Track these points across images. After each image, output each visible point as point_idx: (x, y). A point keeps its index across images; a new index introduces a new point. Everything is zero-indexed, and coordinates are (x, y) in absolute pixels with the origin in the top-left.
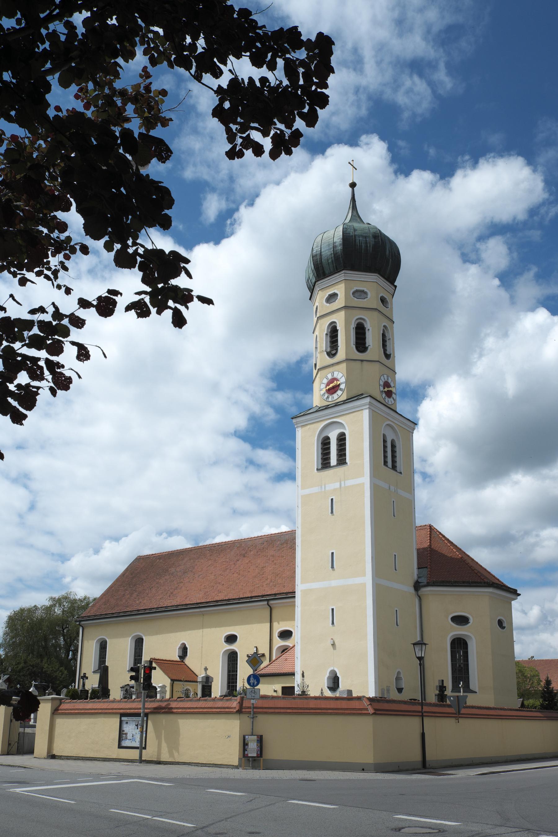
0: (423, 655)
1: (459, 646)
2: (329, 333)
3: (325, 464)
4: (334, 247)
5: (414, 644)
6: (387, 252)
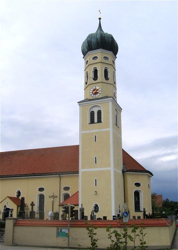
1: (137, 194)
3: (92, 122)
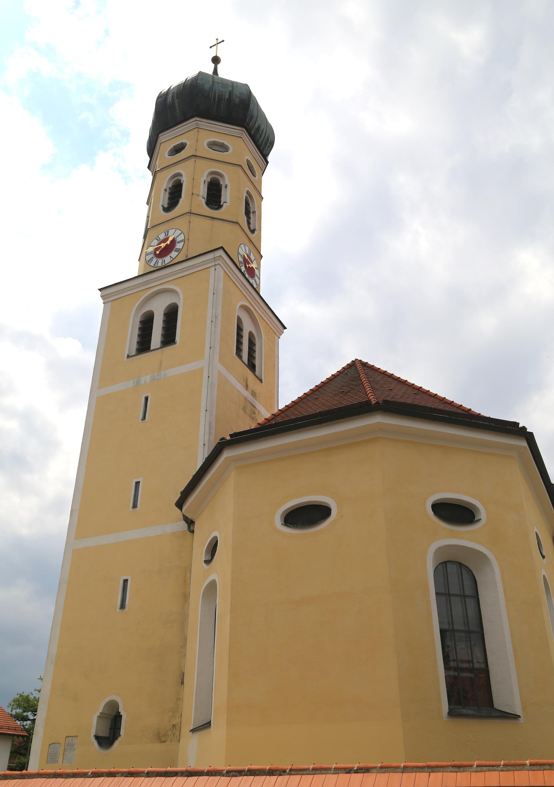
2: (168, 191)
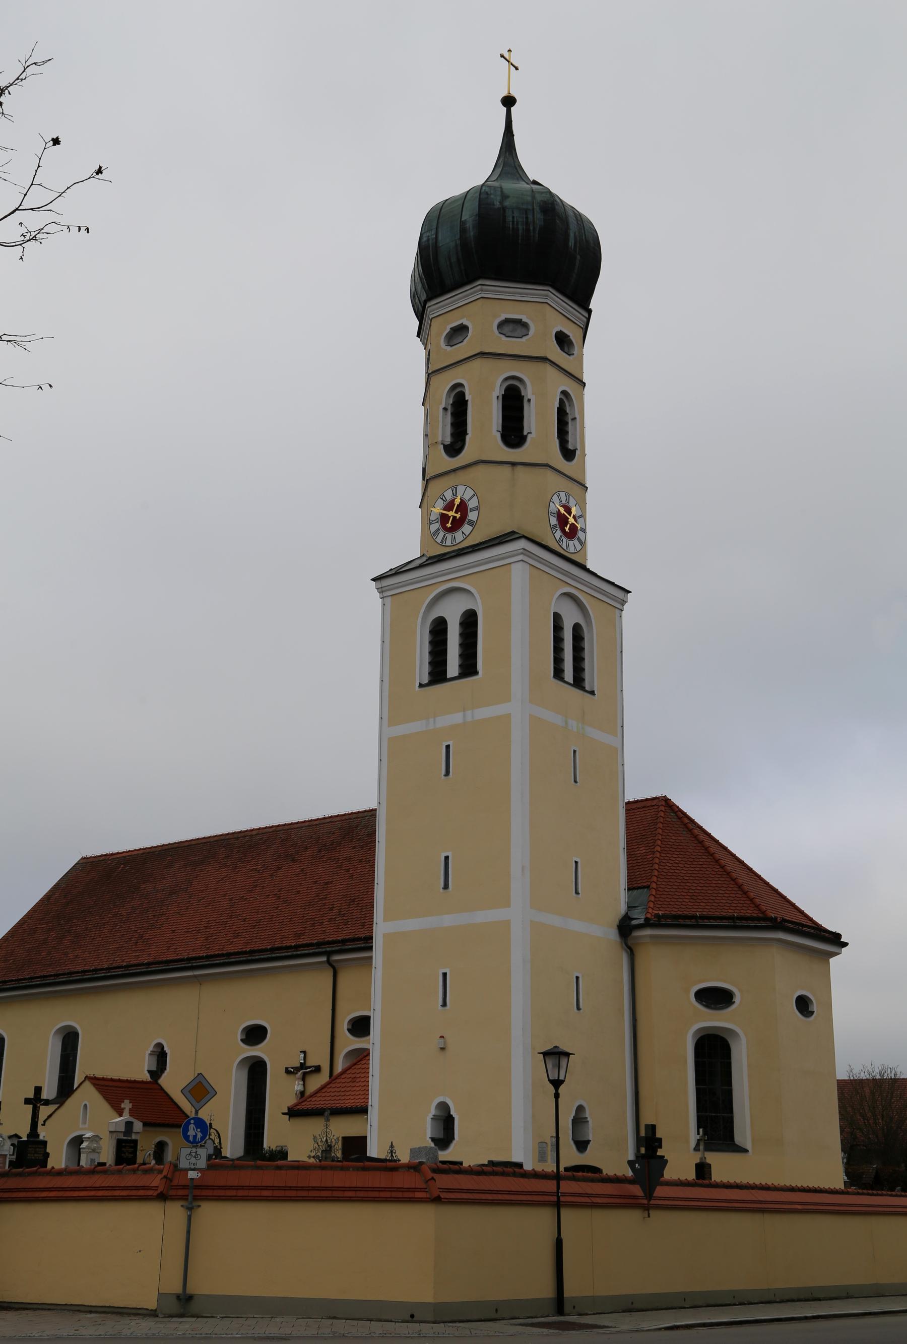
0: (562, 1078)
1: (713, 1054)
2: (449, 408)
3: (438, 674)
4: (463, 230)
5: (546, 1054)
6: (571, 243)
